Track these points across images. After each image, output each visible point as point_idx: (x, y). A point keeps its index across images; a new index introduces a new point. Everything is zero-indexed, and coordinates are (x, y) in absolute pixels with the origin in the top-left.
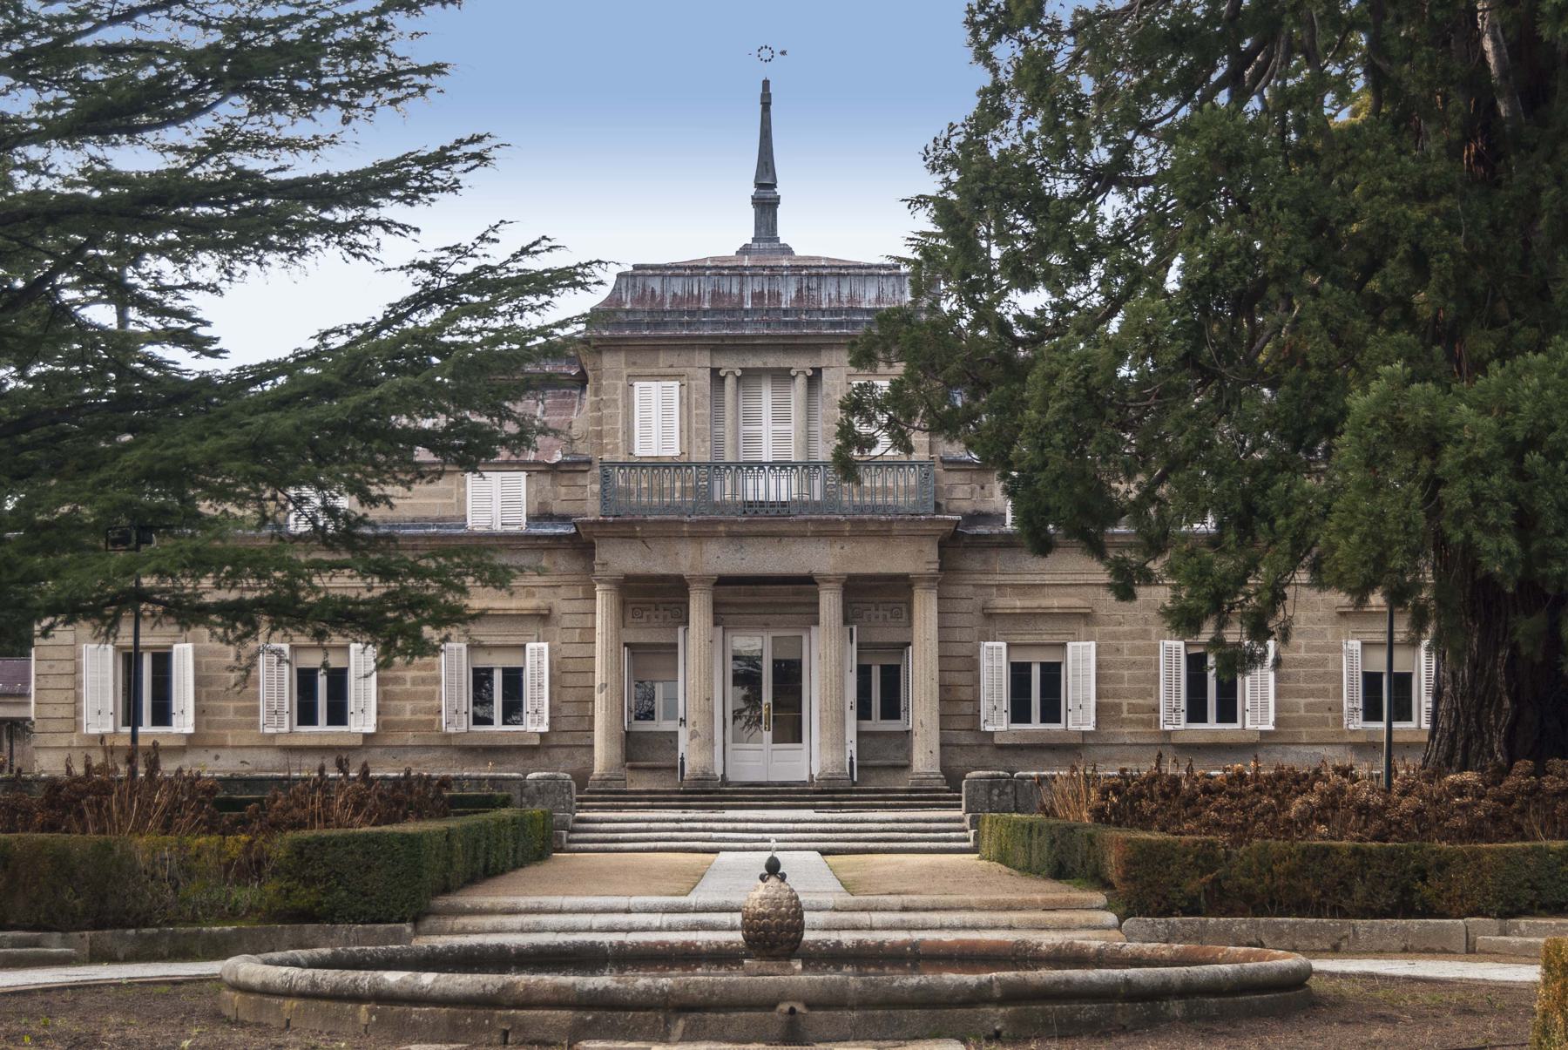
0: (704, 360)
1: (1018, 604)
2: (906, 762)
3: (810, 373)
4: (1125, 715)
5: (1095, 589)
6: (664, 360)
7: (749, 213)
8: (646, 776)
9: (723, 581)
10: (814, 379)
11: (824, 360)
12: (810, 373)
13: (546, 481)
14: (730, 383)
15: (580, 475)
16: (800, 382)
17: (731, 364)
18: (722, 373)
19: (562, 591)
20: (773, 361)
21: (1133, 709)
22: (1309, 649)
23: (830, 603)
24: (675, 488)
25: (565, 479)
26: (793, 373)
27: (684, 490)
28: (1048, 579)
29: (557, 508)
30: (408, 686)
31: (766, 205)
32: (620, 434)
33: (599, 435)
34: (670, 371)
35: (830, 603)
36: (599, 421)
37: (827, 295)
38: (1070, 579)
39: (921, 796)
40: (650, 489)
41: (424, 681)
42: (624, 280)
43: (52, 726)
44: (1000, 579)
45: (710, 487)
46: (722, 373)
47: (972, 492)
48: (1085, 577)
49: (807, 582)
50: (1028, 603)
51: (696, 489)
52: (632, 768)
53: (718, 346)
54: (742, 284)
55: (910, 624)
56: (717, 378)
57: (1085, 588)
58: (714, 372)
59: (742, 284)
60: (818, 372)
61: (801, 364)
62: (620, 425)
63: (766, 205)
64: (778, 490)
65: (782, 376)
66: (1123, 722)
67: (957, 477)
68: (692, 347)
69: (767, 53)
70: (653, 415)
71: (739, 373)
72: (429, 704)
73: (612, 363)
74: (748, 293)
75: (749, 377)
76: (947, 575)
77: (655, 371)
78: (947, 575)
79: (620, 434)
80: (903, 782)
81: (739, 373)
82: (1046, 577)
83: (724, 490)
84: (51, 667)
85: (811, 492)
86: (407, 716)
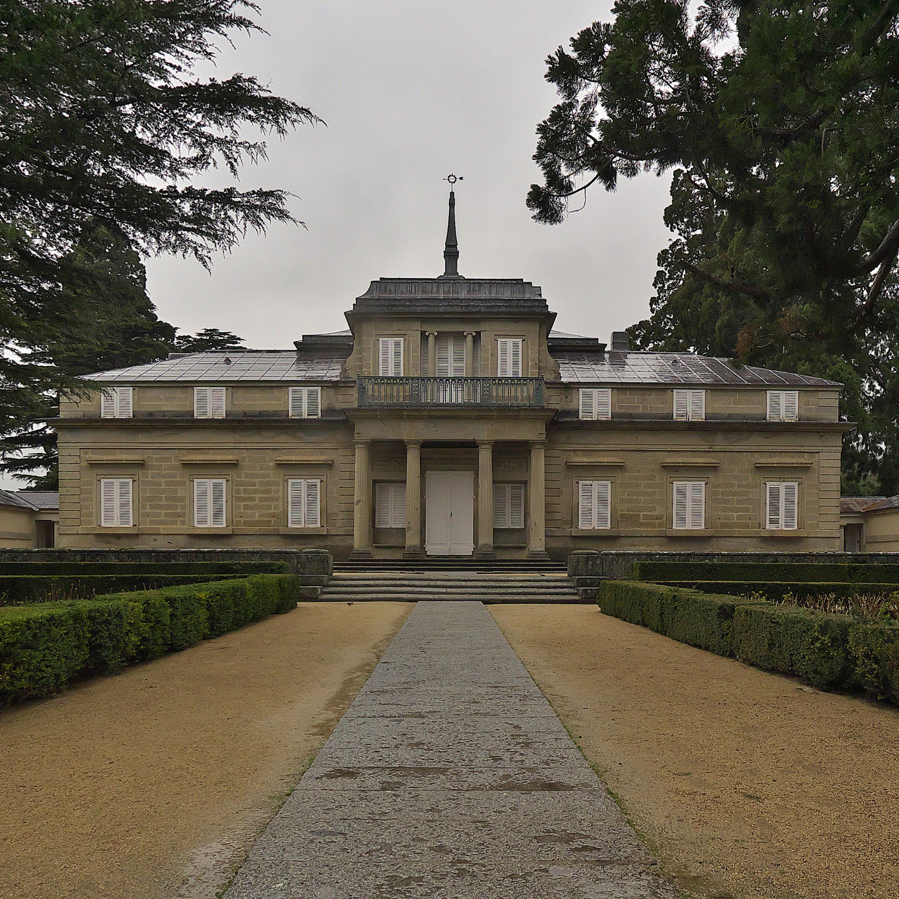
0: (417, 326)
1: (585, 460)
2: (525, 545)
3: (474, 334)
4: (641, 521)
5: (626, 453)
6: (396, 327)
7: (443, 261)
8: (385, 551)
9: (426, 445)
10: (477, 338)
11: (482, 327)
12: (474, 334)
13: (331, 392)
14: (431, 339)
15: (351, 389)
16: (469, 338)
17: (432, 330)
18: (427, 334)
19: (340, 452)
20: (454, 328)
21: (645, 517)
22: (739, 486)
23: (485, 456)
24: (400, 395)
25: (342, 391)
26: (465, 334)
27: (405, 397)
28: (601, 447)
29: (339, 406)
30: (257, 502)
31: (451, 254)
32: (371, 366)
33: (361, 367)
34: (400, 332)
35: (485, 456)
36: (360, 360)
37: (484, 294)
38: (613, 447)
39: (534, 564)
40: (386, 396)
41: (265, 499)
42: (375, 284)
43: (69, 522)
44: (576, 447)
45: (419, 396)
46: (427, 334)
47: (561, 399)
48: (621, 446)
49: (472, 445)
50: (590, 460)
51: (411, 397)
52: (377, 547)
53: (426, 318)
54: (438, 287)
55: (528, 468)
56: (424, 337)
57: (620, 452)
58: (423, 333)
59: (438, 287)
60: (479, 333)
61: (469, 329)
62: (371, 361)
63: (451, 254)
64: (457, 399)
65: (459, 337)
66: (641, 525)
67: (553, 392)
68: (410, 319)
69: (452, 179)
70: (389, 356)
71: (436, 334)
72: (268, 512)
73: (368, 328)
74: (441, 291)
75: (441, 337)
76: (549, 444)
77: (391, 332)
78: (549, 444)
79: (371, 366)
80: (523, 555)
81: (436, 334)
82: (600, 446)
83: (426, 398)
84: (67, 491)
85: (475, 399)
86: (257, 518)
